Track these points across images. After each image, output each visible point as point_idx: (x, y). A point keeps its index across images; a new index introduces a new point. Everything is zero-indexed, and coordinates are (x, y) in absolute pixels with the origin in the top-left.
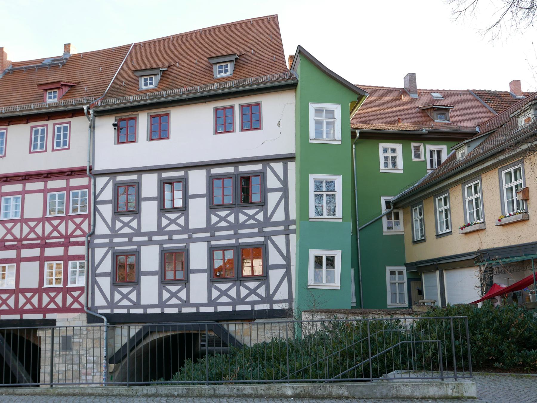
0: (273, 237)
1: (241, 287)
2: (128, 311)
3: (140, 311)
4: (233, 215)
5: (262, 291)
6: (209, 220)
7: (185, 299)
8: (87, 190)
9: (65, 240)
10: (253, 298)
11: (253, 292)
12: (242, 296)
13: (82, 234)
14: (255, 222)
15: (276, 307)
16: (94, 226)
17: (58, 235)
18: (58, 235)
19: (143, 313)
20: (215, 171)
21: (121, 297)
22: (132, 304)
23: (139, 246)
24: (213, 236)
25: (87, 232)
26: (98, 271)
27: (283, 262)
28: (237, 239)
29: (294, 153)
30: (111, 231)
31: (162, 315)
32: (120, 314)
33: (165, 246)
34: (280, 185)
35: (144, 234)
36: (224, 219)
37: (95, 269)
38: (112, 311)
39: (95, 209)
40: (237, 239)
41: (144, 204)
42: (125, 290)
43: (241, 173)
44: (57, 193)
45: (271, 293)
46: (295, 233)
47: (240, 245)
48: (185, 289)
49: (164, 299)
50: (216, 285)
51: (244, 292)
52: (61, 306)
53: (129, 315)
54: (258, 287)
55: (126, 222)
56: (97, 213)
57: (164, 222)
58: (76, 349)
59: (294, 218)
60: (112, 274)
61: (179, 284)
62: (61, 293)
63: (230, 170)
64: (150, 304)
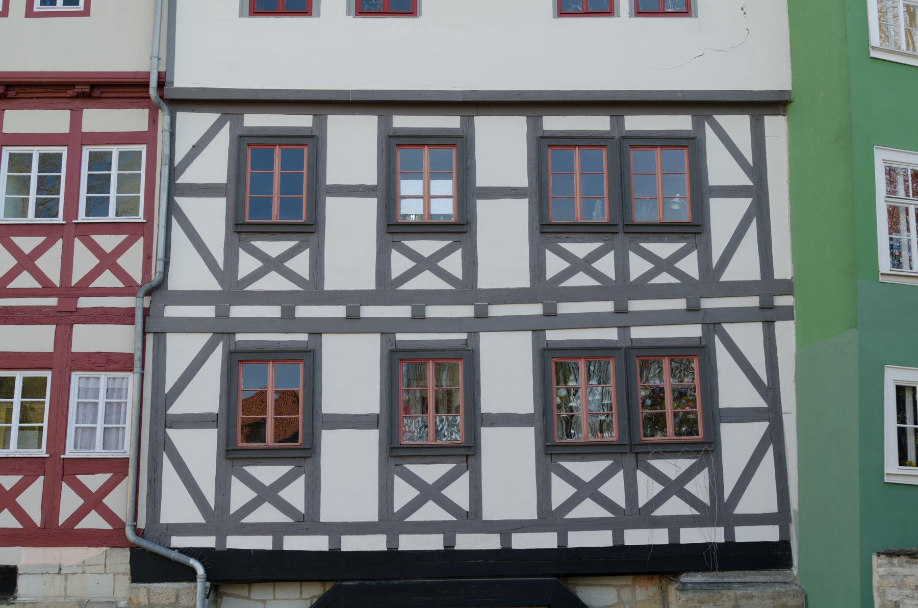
0: (727, 327)
2: (278, 541)
3: (319, 543)
4: (611, 255)
5: (699, 487)
6: (537, 266)
7: (465, 505)
8: (143, 148)
9: (59, 302)
10: (675, 507)
12: (643, 500)
13: (119, 284)
14: (674, 280)
15: (744, 534)
16: (167, 264)
17: (34, 284)
18: (34, 284)
19: (327, 550)
20: (553, 123)
21: (254, 495)
22: (289, 520)
23: (316, 334)
24: (550, 314)
25: (139, 282)
26: (177, 408)
27: (759, 402)
28: (624, 329)
29: (789, 92)
30: (221, 283)
31: (392, 556)
33: (400, 337)
36: (585, 265)
37: (163, 400)
38: (221, 540)
39: (172, 209)
40: (624, 329)
41: (333, 206)
42: (267, 474)
43: (630, 135)
44: (36, 152)
46: (792, 319)
47: (634, 345)
49: (397, 506)
52: (38, 523)
54: (689, 475)
55: (274, 256)
56: (175, 223)
57: (399, 264)
59: (788, 276)
60: (222, 421)
61: (446, 459)
62: (41, 479)
63: (599, 123)
64: (350, 520)
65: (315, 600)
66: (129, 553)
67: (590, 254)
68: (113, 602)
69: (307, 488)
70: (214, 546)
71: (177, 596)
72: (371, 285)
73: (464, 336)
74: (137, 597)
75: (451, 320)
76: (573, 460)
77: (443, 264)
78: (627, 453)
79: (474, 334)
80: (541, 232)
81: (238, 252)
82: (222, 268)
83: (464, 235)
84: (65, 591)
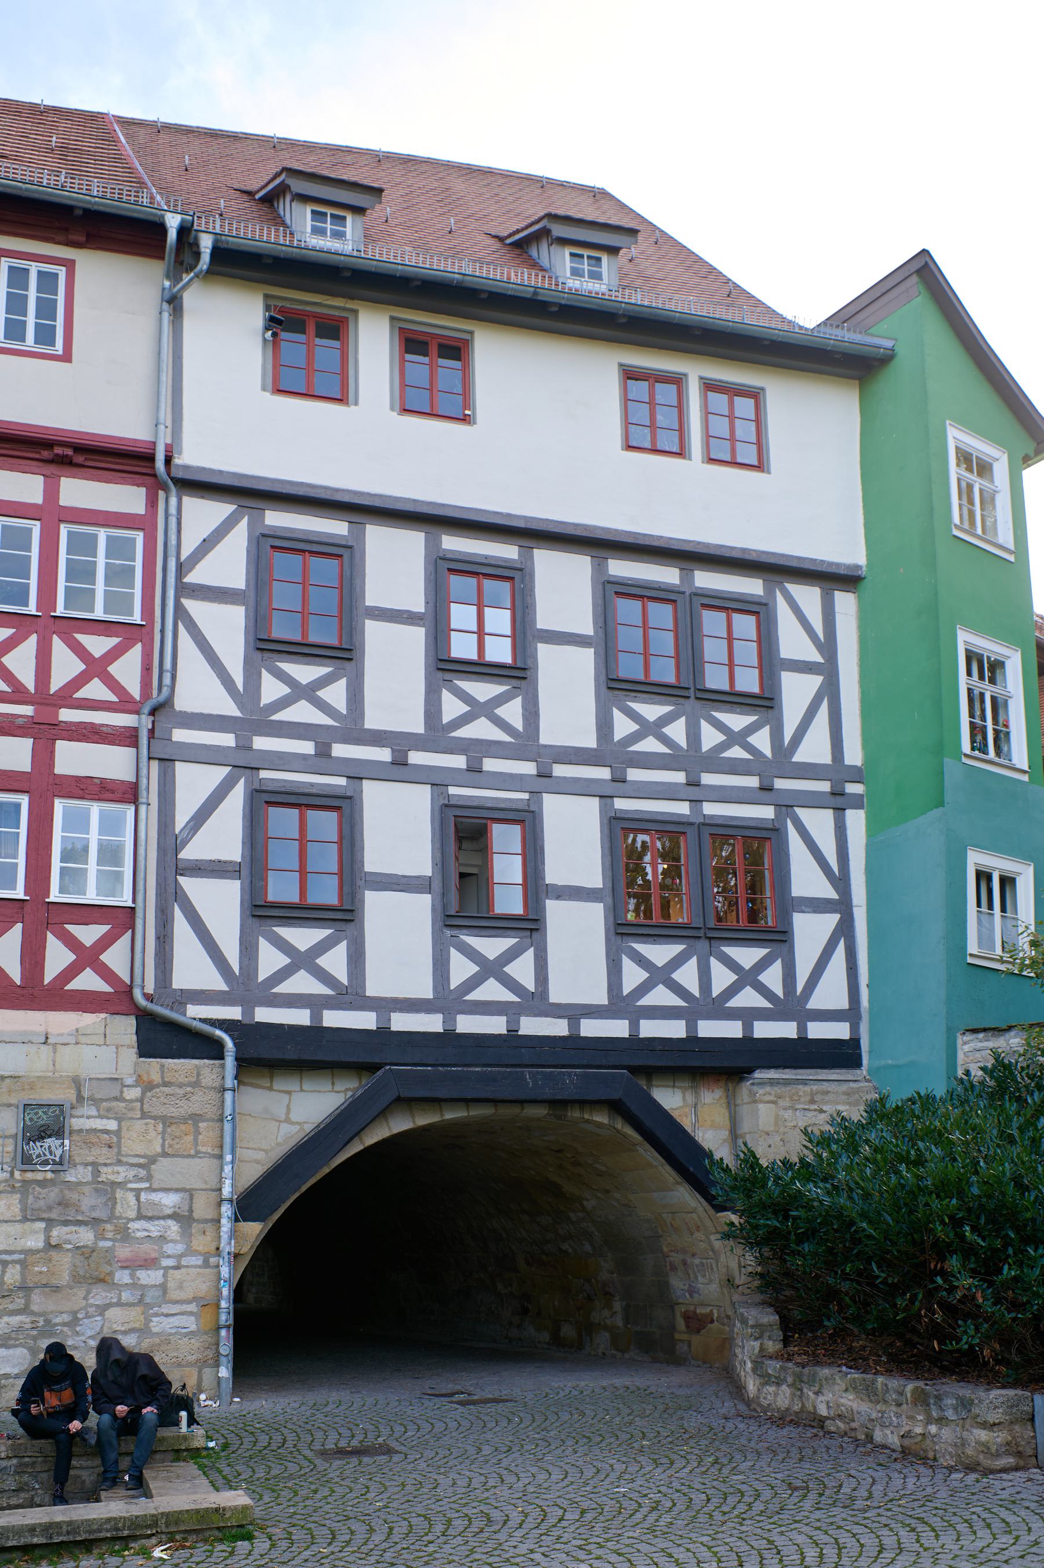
0: (797, 810)
1: (713, 960)
2: (316, 1016)
4: (682, 720)
5: (773, 977)
7: (530, 985)
10: (748, 998)
11: (748, 978)
12: (716, 991)
14: (745, 755)
15: (817, 1031)
24: (619, 779)
31: (449, 1037)
32: (282, 1025)
33: (453, 790)
34: (814, 656)
35: (377, 738)
36: (654, 729)
38: (248, 1011)
40: (696, 802)
45: (800, 987)
47: (707, 821)
48: (531, 950)
50: (636, 946)
51: (722, 978)
53: (316, 1032)
55: (304, 683)
57: (451, 707)
58: (90, 1159)
60: (245, 872)
61: (509, 932)
64: (401, 996)
65: (350, 1094)
66: (134, 1022)
67: (660, 718)
68: (116, 1079)
69: (350, 957)
70: (240, 1019)
71: (198, 1075)
72: (420, 729)
73: (526, 796)
74: (148, 1074)
75: (512, 776)
76: (645, 943)
77: (501, 712)
78: (699, 937)
79: (536, 794)
80: (609, 688)
81: (260, 673)
82: (241, 690)
83: (523, 682)
84: (54, 1065)
